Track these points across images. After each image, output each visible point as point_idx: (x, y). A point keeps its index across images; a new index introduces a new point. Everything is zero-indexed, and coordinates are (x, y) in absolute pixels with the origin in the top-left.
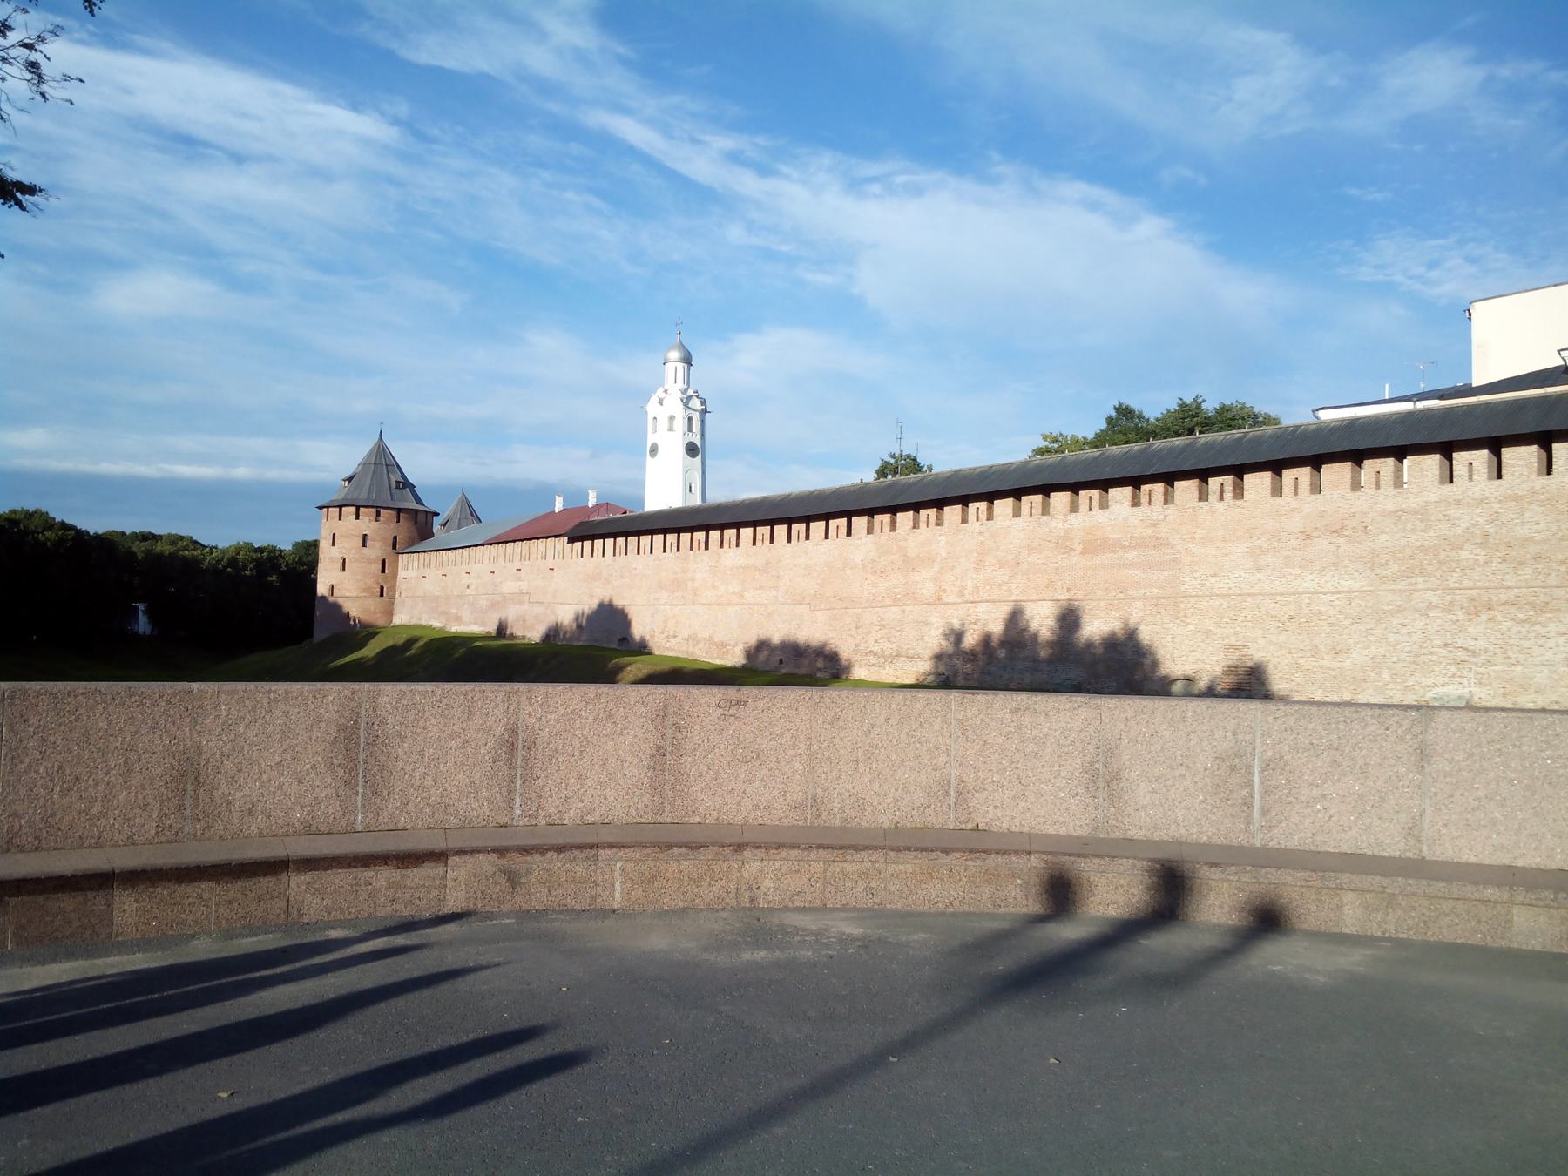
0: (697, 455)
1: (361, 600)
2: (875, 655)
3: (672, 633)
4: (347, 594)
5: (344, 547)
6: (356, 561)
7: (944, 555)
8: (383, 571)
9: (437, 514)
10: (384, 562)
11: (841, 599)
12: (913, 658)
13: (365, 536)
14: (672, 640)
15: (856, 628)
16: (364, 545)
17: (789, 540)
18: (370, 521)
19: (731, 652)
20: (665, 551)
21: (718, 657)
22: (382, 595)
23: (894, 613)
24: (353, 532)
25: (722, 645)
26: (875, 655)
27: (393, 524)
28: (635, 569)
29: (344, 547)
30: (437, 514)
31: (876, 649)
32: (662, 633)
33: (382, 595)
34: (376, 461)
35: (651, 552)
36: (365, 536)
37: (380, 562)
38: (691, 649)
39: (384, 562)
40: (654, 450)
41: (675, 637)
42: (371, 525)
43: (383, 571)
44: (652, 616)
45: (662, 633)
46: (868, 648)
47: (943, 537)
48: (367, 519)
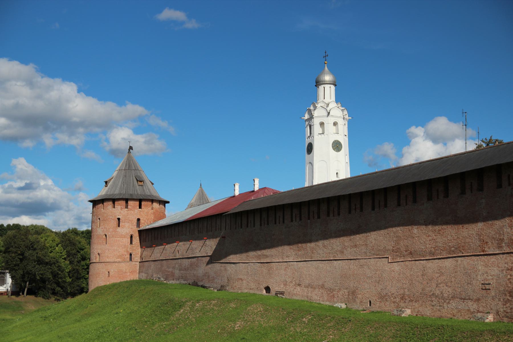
0: (341, 150)
1: (117, 264)
2: (436, 297)
3: (297, 282)
4: (108, 260)
5: (105, 228)
6: (113, 236)
7: (485, 214)
8: (131, 243)
9: (168, 202)
10: (131, 237)
11: (411, 253)
12: (464, 299)
13: (119, 219)
14: (298, 288)
15: (422, 275)
16: (119, 226)
17: (373, 209)
18: (121, 208)
19: (336, 296)
20: (292, 221)
21: (328, 300)
22: (131, 259)
23: (448, 263)
24: (111, 217)
25: (331, 290)
26: (436, 297)
27: (137, 210)
28: (274, 234)
29: (105, 228)
30: (168, 202)
31: (437, 292)
32: (291, 282)
33: (131, 259)
34: (125, 168)
35: (284, 222)
36: (119, 219)
37: (129, 237)
38: (310, 294)
39: (131, 237)
40: (310, 148)
41: (299, 285)
42: (122, 212)
43: (131, 243)
44: (285, 270)
45: (291, 282)
46: (431, 291)
47: (483, 201)
48: (119, 207)
